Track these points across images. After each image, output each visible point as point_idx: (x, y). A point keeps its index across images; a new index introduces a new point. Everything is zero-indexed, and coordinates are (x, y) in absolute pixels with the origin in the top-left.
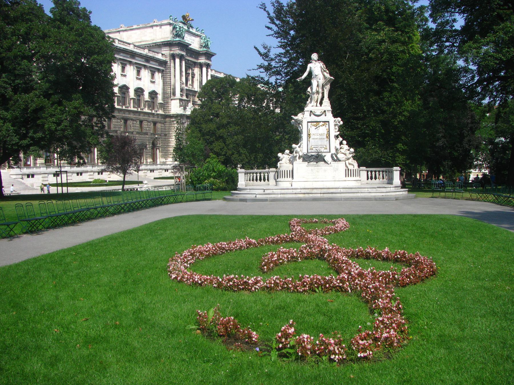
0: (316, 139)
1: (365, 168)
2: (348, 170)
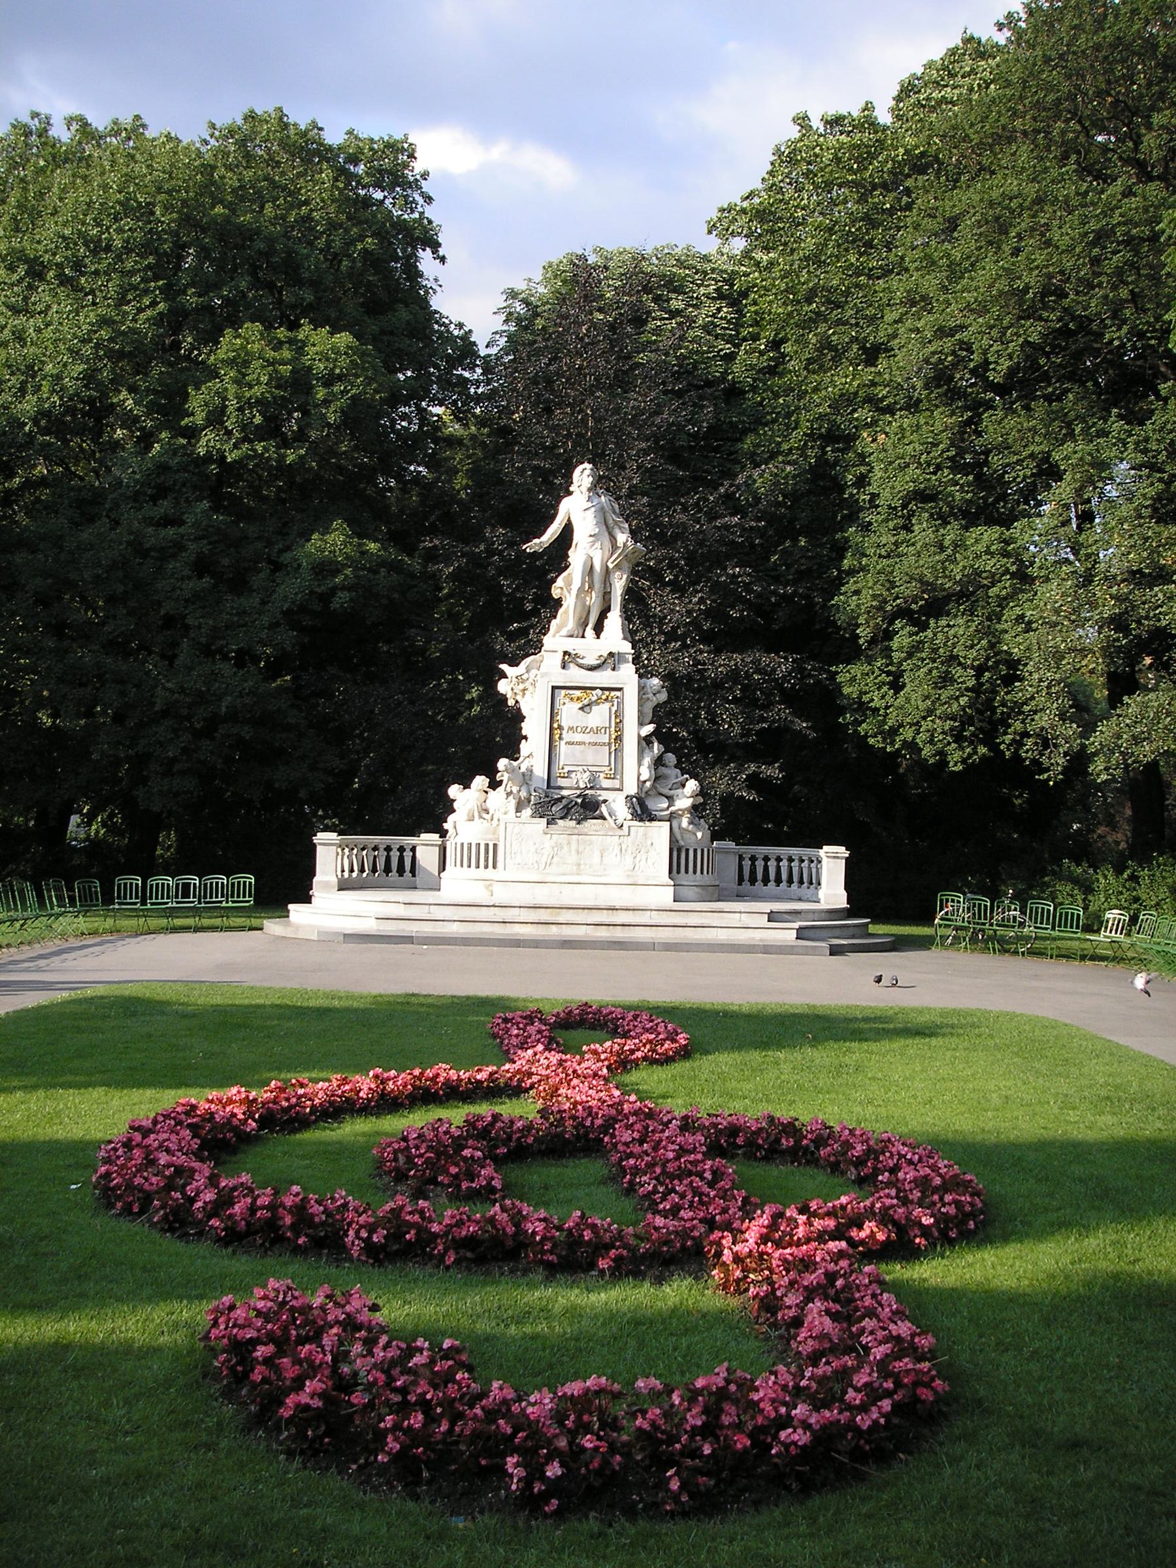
1: (732, 845)
2: (679, 851)
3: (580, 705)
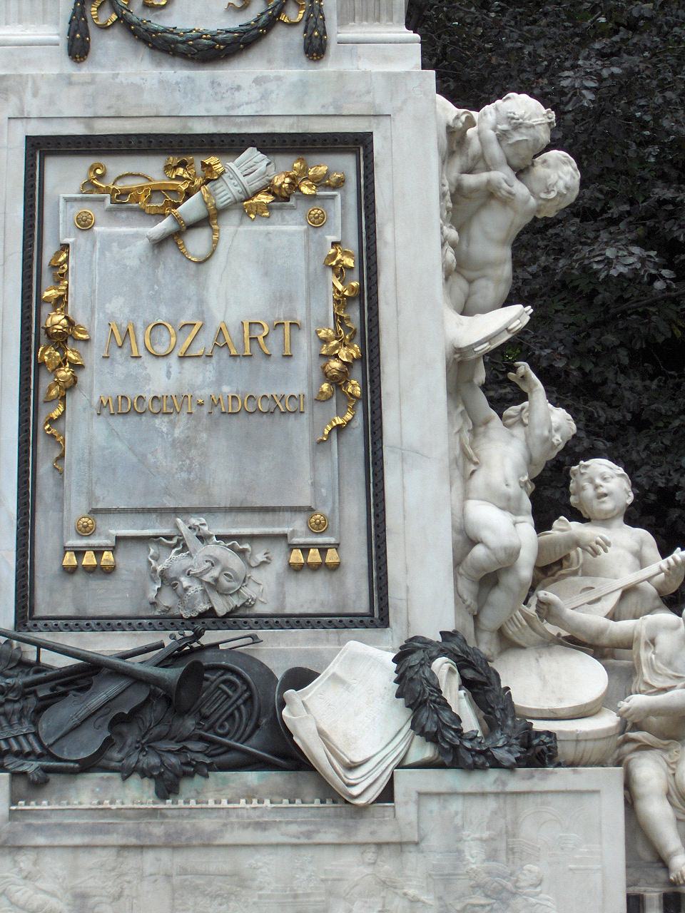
0: (165, 407)
3: (165, 225)
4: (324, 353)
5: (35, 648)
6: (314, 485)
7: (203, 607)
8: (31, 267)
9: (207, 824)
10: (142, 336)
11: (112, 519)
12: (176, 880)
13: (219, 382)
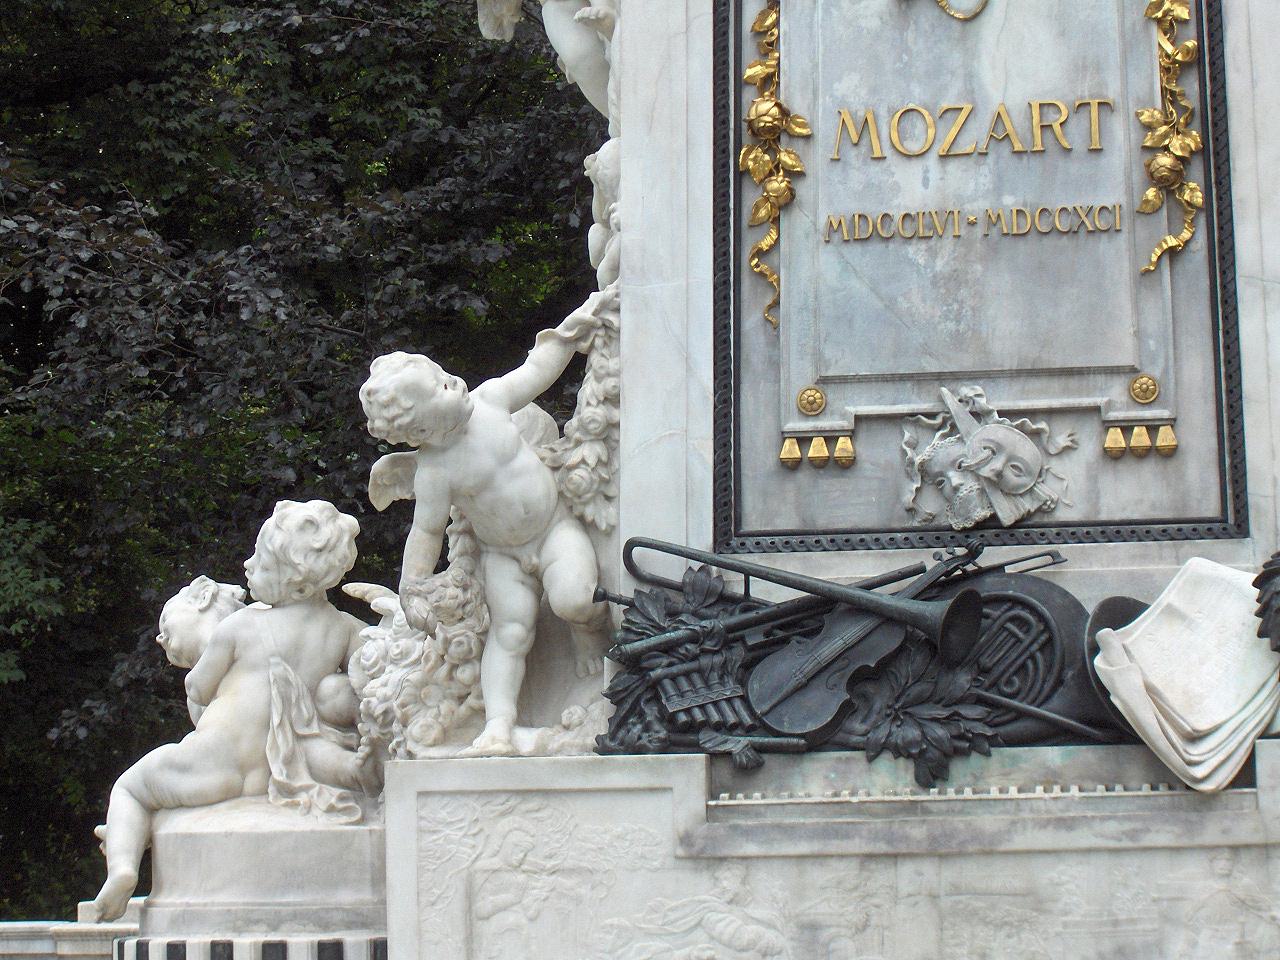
0: (921, 228)
4: (1148, 144)
5: (743, 576)
6: (1139, 334)
7: (981, 513)
8: (726, 33)
9: (988, 822)
10: (887, 128)
11: (849, 390)
12: (946, 902)
13: (998, 190)
